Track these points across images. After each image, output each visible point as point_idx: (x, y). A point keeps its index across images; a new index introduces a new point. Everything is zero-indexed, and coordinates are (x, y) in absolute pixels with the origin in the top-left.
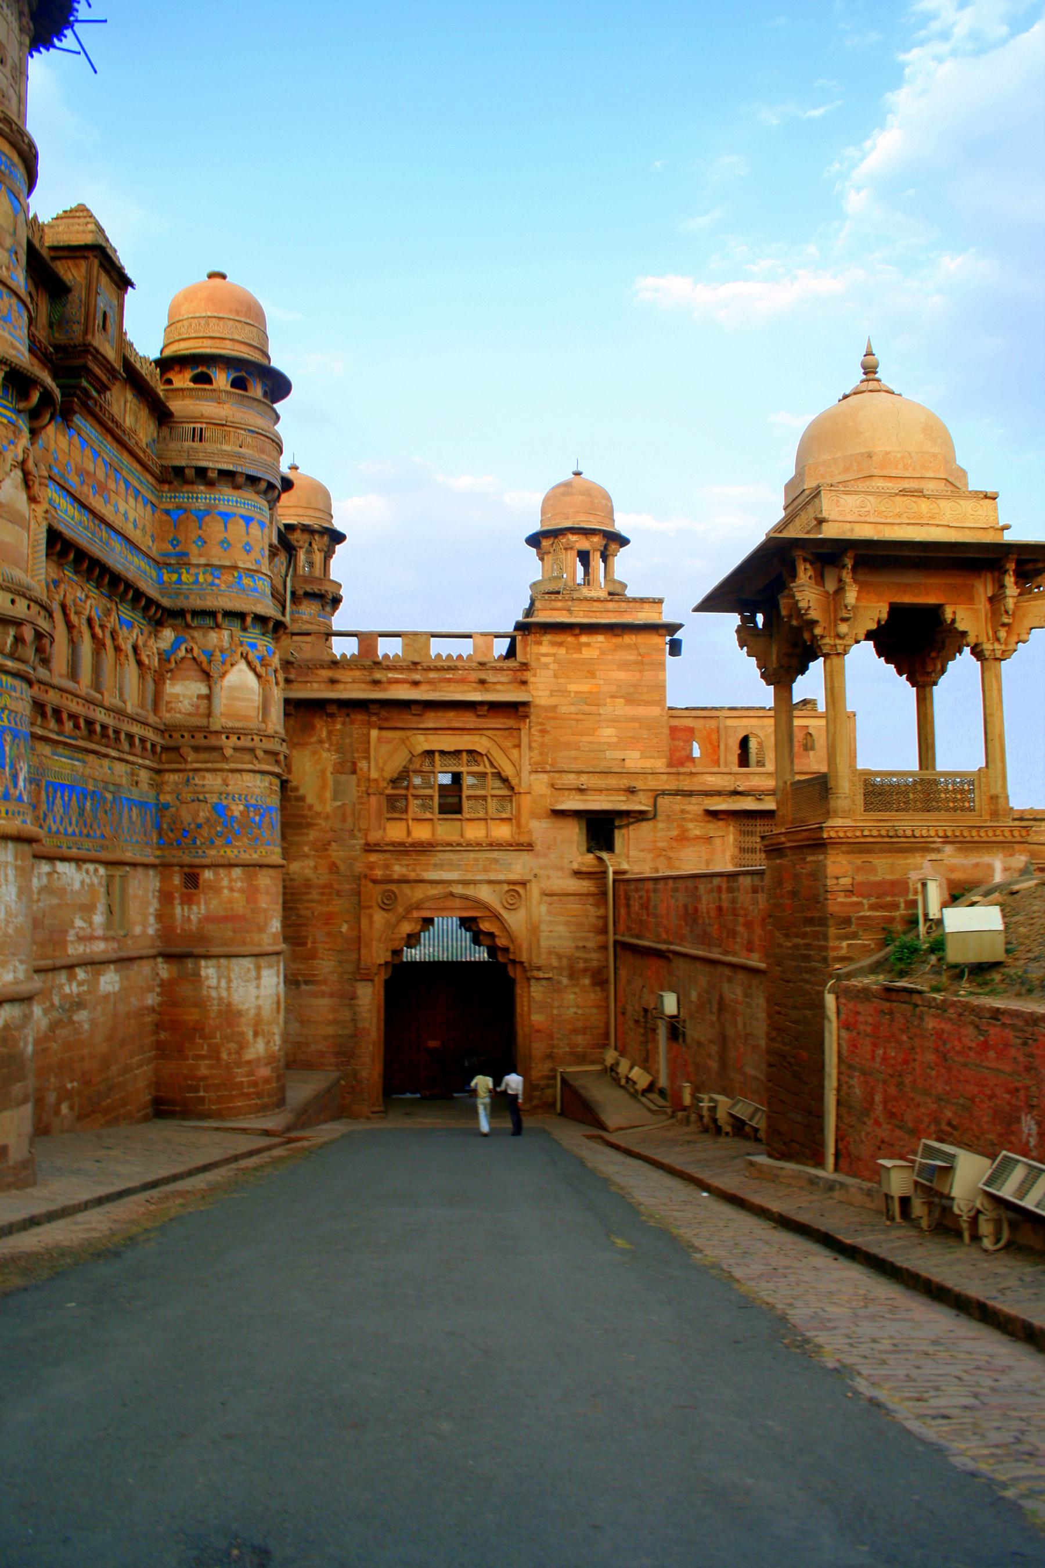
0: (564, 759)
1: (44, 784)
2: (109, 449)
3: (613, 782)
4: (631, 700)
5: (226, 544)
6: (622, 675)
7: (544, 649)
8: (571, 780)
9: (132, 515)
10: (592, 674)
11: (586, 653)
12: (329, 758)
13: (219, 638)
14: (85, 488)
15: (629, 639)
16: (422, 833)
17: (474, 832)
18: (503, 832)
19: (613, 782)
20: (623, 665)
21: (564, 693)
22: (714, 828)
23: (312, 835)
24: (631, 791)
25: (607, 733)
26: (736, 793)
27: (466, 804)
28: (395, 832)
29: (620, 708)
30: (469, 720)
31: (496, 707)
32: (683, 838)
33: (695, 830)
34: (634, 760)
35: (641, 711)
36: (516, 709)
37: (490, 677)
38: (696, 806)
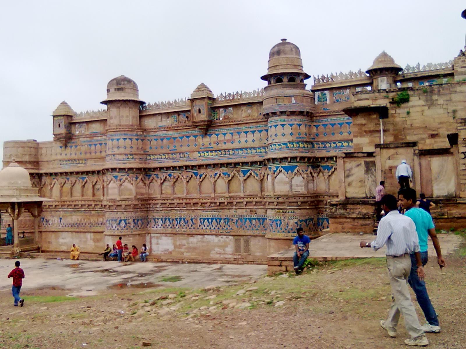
1: (199, 219)
2: (232, 129)
14: (219, 145)
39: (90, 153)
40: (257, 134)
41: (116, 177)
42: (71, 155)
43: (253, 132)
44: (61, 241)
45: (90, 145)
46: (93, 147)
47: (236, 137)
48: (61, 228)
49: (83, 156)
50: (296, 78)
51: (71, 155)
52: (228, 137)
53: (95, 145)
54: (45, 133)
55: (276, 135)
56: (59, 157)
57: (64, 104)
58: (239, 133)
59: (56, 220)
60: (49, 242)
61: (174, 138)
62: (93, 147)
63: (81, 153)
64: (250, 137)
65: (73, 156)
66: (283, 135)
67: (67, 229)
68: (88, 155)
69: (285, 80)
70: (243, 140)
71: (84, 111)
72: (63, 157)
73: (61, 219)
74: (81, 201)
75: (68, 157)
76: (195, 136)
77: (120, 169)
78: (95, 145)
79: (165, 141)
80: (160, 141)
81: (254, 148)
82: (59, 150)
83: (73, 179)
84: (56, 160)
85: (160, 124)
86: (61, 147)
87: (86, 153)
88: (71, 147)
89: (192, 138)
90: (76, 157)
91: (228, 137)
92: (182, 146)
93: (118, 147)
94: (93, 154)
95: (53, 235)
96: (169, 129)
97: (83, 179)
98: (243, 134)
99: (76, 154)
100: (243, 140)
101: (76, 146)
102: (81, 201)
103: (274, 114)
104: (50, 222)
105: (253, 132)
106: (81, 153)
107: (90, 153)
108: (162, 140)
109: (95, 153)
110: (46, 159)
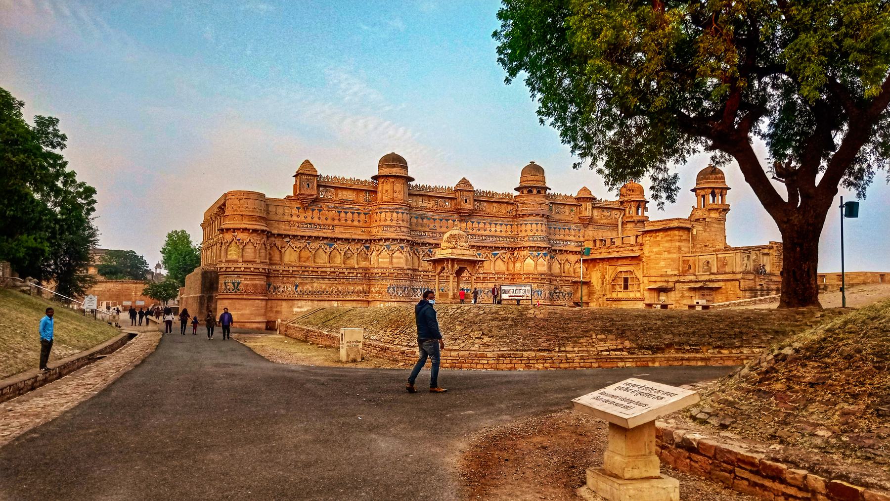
0: (653, 272)
3: (663, 279)
4: (669, 252)
5: (526, 231)
6: (667, 245)
7: (648, 238)
8: (653, 279)
9: (499, 230)
10: (659, 245)
11: (658, 238)
12: (600, 274)
13: (525, 253)
15: (669, 233)
16: (620, 295)
17: (632, 295)
18: (638, 295)
19: (663, 279)
20: (667, 241)
21: (652, 251)
22: (692, 294)
23: (596, 296)
24: (668, 282)
25: (662, 264)
26: (696, 282)
27: (630, 287)
28: (614, 295)
29: (666, 255)
30: (628, 262)
31: (633, 258)
32: (683, 297)
33: (687, 294)
34: (670, 272)
35: (671, 256)
36: (637, 258)
37: (634, 248)
38: (687, 286)
39: (339, 220)
40: (504, 227)
41: (388, 248)
42: (312, 218)
43: (501, 225)
44: (296, 309)
45: (339, 212)
46: (343, 215)
47: (488, 226)
48: (296, 296)
49: (329, 222)
50: (542, 189)
51: (312, 218)
52: (482, 225)
53: (346, 213)
54: (281, 188)
55: (537, 230)
56: (295, 218)
57: (307, 161)
58: (490, 224)
59: (290, 287)
60: (277, 312)
61: (434, 220)
62: (343, 215)
63: (327, 219)
64: (498, 228)
65: (316, 220)
66: (531, 231)
67: (305, 297)
68: (336, 222)
69: (535, 191)
70: (493, 229)
71: (331, 175)
72: (302, 219)
73: (297, 286)
74: (330, 267)
75: (309, 220)
76: (454, 221)
77: (393, 239)
78: (346, 213)
79: (425, 220)
80: (420, 220)
81: (502, 237)
82: (295, 211)
83: (315, 244)
84: (297, 219)
85: (420, 204)
86: (298, 208)
87: (333, 219)
88: (313, 210)
89: (450, 221)
90: (320, 222)
91: (482, 225)
92: (441, 227)
93: (403, 221)
94: (349, 222)
95: (284, 304)
96: (431, 210)
97: (331, 246)
98: (493, 225)
99: (319, 218)
100: (493, 229)
101: (320, 211)
102: (330, 267)
103: (537, 215)
104: (281, 289)
105: (501, 225)
106: (327, 219)
107: (339, 220)
108: (422, 219)
109: (346, 220)
110: (277, 218)
